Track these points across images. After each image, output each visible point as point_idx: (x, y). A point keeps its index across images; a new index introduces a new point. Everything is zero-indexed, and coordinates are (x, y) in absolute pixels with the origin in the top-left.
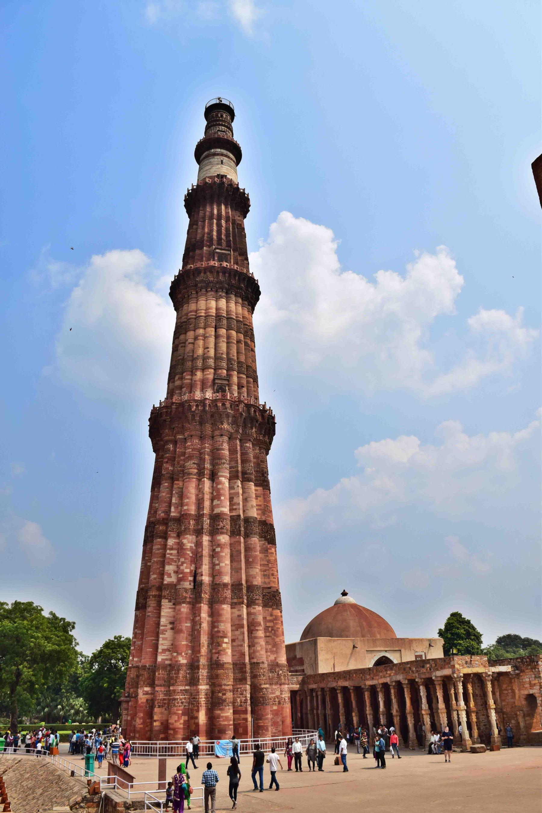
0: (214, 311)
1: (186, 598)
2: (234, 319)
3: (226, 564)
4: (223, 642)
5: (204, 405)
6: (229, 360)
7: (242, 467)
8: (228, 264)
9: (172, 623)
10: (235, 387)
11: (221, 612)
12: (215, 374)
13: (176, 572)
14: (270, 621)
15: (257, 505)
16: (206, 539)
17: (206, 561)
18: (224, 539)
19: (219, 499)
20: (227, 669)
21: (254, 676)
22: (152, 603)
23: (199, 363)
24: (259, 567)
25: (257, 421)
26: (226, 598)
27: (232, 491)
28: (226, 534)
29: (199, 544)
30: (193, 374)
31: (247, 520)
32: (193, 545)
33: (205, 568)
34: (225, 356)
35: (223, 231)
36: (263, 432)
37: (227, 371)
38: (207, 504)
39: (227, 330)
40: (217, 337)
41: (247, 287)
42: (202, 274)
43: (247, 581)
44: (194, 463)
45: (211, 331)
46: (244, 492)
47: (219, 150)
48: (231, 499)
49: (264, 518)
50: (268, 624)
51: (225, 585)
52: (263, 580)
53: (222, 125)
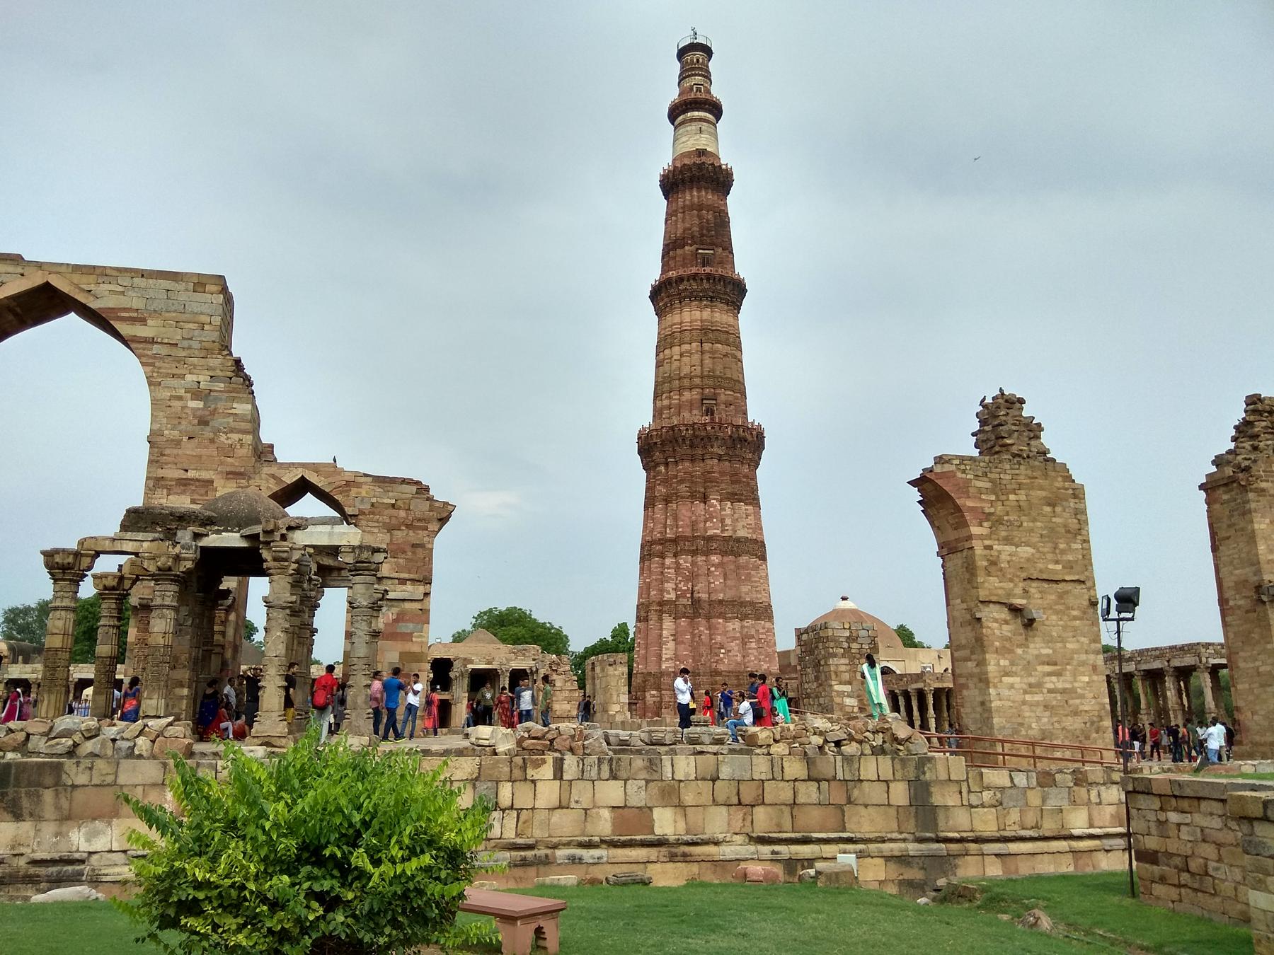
6: (714, 377)
13: (675, 589)
17: (702, 579)
22: (653, 616)
23: (686, 382)
31: (738, 540)
40: (702, 353)
47: (696, 113)
51: (721, 602)
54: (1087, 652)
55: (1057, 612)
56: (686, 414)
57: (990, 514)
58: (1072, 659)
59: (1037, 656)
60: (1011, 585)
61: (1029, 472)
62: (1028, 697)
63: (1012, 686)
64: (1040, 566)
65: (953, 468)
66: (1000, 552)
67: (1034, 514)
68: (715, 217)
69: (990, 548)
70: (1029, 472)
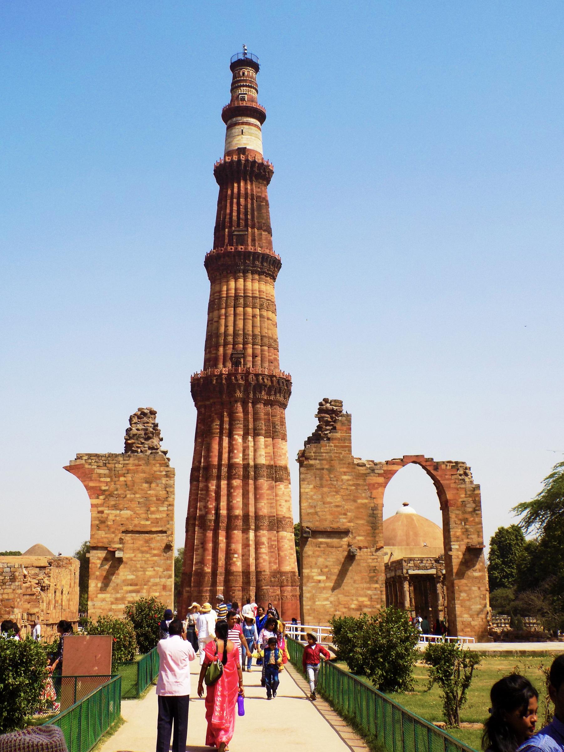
0: (233, 291)
1: (210, 526)
2: (249, 297)
3: (237, 501)
4: (234, 557)
5: (222, 379)
6: (245, 335)
7: (254, 425)
8: (243, 247)
9: (202, 543)
10: (250, 359)
11: (233, 536)
12: (233, 348)
14: (274, 541)
15: (266, 453)
16: (224, 483)
18: (237, 482)
19: (233, 452)
20: (236, 576)
21: (258, 580)
24: (265, 502)
25: (266, 386)
26: (237, 526)
27: (245, 445)
28: (238, 478)
29: (218, 486)
30: (217, 350)
31: (256, 466)
32: (214, 487)
33: (223, 504)
34: (241, 332)
35: (242, 210)
36: (273, 392)
37: (243, 345)
38: (225, 456)
39: (244, 308)
40: (235, 315)
41: (262, 263)
42: (222, 259)
43: (256, 513)
44: (217, 425)
45: (231, 311)
46: (254, 444)
48: (244, 451)
49: (272, 463)
50: (273, 543)
51: (237, 517)
52: (270, 510)
53: (243, 86)
54: (160, 577)
55: (142, 552)
56: (221, 366)
57: (105, 491)
58: (149, 581)
59: (124, 581)
60: (113, 535)
61: (136, 462)
62: (114, 607)
63: (103, 600)
64: (136, 522)
65: (83, 462)
66: (108, 515)
67: (136, 488)
68: (252, 204)
69: (102, 512)
70: (136, 462)
